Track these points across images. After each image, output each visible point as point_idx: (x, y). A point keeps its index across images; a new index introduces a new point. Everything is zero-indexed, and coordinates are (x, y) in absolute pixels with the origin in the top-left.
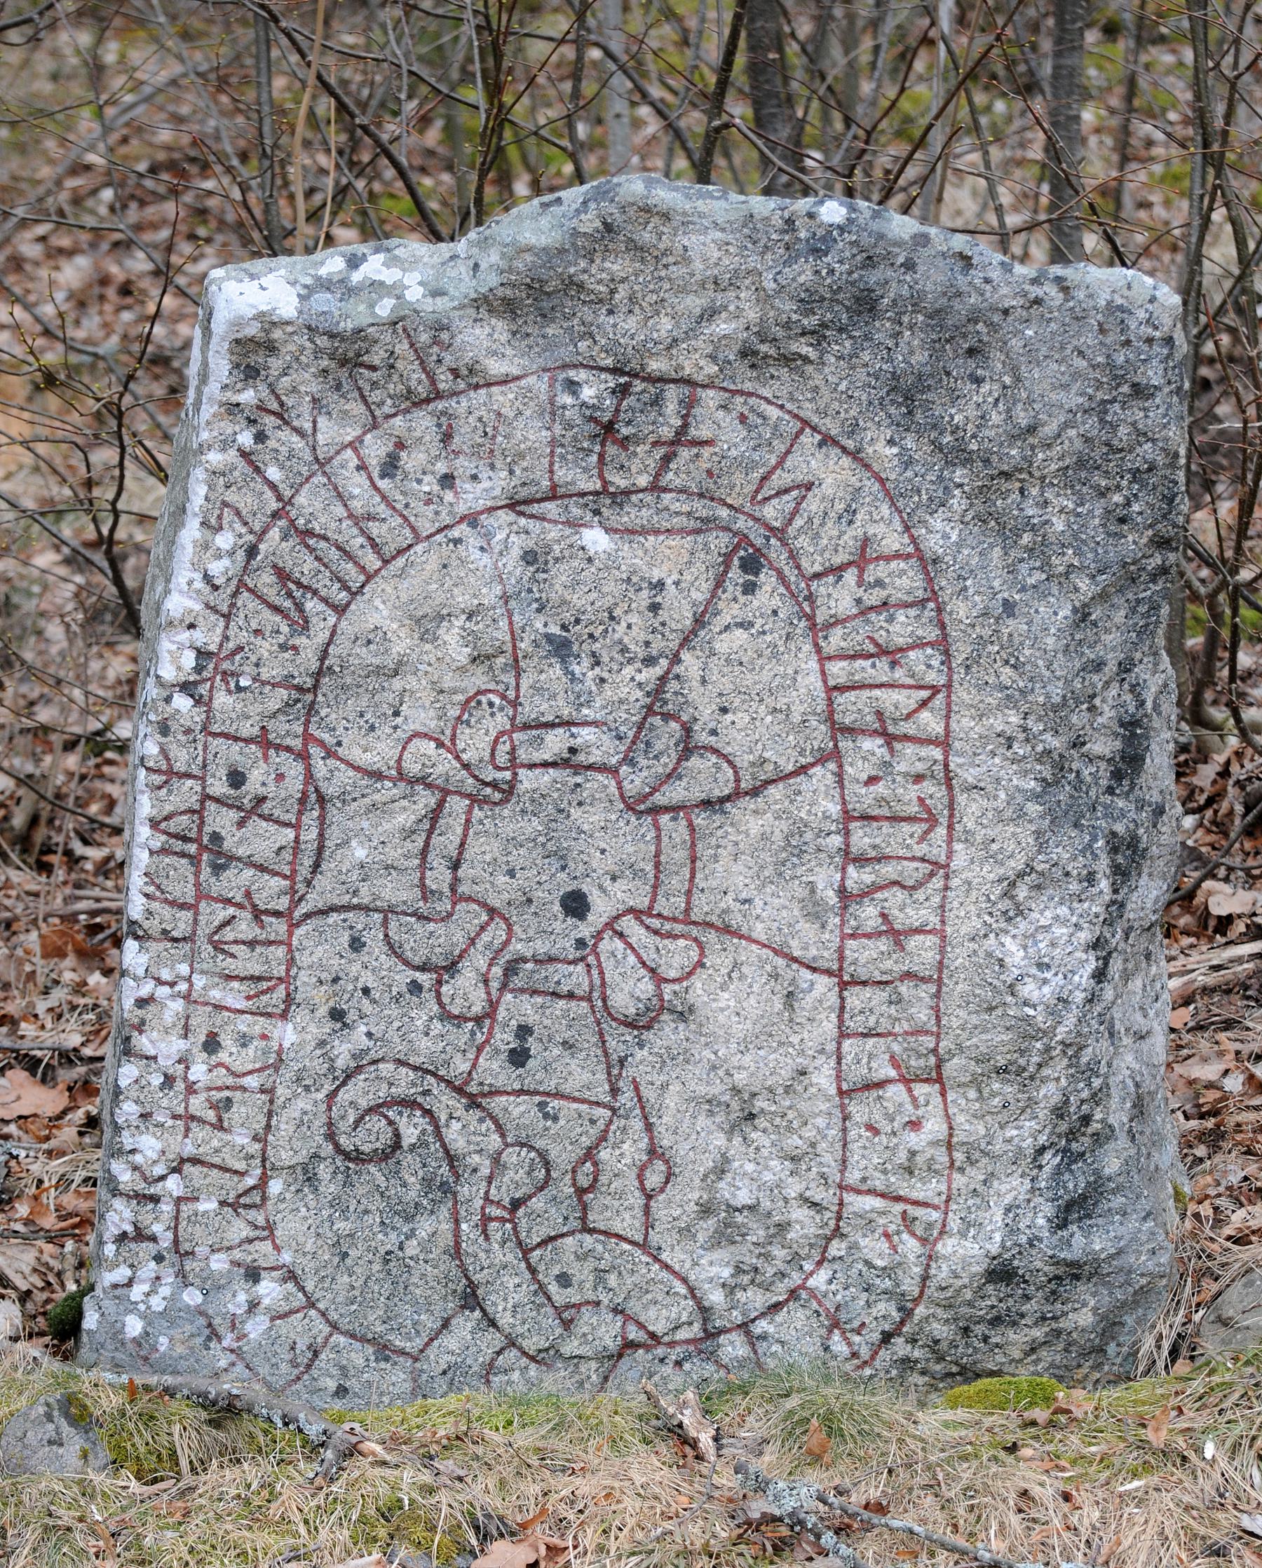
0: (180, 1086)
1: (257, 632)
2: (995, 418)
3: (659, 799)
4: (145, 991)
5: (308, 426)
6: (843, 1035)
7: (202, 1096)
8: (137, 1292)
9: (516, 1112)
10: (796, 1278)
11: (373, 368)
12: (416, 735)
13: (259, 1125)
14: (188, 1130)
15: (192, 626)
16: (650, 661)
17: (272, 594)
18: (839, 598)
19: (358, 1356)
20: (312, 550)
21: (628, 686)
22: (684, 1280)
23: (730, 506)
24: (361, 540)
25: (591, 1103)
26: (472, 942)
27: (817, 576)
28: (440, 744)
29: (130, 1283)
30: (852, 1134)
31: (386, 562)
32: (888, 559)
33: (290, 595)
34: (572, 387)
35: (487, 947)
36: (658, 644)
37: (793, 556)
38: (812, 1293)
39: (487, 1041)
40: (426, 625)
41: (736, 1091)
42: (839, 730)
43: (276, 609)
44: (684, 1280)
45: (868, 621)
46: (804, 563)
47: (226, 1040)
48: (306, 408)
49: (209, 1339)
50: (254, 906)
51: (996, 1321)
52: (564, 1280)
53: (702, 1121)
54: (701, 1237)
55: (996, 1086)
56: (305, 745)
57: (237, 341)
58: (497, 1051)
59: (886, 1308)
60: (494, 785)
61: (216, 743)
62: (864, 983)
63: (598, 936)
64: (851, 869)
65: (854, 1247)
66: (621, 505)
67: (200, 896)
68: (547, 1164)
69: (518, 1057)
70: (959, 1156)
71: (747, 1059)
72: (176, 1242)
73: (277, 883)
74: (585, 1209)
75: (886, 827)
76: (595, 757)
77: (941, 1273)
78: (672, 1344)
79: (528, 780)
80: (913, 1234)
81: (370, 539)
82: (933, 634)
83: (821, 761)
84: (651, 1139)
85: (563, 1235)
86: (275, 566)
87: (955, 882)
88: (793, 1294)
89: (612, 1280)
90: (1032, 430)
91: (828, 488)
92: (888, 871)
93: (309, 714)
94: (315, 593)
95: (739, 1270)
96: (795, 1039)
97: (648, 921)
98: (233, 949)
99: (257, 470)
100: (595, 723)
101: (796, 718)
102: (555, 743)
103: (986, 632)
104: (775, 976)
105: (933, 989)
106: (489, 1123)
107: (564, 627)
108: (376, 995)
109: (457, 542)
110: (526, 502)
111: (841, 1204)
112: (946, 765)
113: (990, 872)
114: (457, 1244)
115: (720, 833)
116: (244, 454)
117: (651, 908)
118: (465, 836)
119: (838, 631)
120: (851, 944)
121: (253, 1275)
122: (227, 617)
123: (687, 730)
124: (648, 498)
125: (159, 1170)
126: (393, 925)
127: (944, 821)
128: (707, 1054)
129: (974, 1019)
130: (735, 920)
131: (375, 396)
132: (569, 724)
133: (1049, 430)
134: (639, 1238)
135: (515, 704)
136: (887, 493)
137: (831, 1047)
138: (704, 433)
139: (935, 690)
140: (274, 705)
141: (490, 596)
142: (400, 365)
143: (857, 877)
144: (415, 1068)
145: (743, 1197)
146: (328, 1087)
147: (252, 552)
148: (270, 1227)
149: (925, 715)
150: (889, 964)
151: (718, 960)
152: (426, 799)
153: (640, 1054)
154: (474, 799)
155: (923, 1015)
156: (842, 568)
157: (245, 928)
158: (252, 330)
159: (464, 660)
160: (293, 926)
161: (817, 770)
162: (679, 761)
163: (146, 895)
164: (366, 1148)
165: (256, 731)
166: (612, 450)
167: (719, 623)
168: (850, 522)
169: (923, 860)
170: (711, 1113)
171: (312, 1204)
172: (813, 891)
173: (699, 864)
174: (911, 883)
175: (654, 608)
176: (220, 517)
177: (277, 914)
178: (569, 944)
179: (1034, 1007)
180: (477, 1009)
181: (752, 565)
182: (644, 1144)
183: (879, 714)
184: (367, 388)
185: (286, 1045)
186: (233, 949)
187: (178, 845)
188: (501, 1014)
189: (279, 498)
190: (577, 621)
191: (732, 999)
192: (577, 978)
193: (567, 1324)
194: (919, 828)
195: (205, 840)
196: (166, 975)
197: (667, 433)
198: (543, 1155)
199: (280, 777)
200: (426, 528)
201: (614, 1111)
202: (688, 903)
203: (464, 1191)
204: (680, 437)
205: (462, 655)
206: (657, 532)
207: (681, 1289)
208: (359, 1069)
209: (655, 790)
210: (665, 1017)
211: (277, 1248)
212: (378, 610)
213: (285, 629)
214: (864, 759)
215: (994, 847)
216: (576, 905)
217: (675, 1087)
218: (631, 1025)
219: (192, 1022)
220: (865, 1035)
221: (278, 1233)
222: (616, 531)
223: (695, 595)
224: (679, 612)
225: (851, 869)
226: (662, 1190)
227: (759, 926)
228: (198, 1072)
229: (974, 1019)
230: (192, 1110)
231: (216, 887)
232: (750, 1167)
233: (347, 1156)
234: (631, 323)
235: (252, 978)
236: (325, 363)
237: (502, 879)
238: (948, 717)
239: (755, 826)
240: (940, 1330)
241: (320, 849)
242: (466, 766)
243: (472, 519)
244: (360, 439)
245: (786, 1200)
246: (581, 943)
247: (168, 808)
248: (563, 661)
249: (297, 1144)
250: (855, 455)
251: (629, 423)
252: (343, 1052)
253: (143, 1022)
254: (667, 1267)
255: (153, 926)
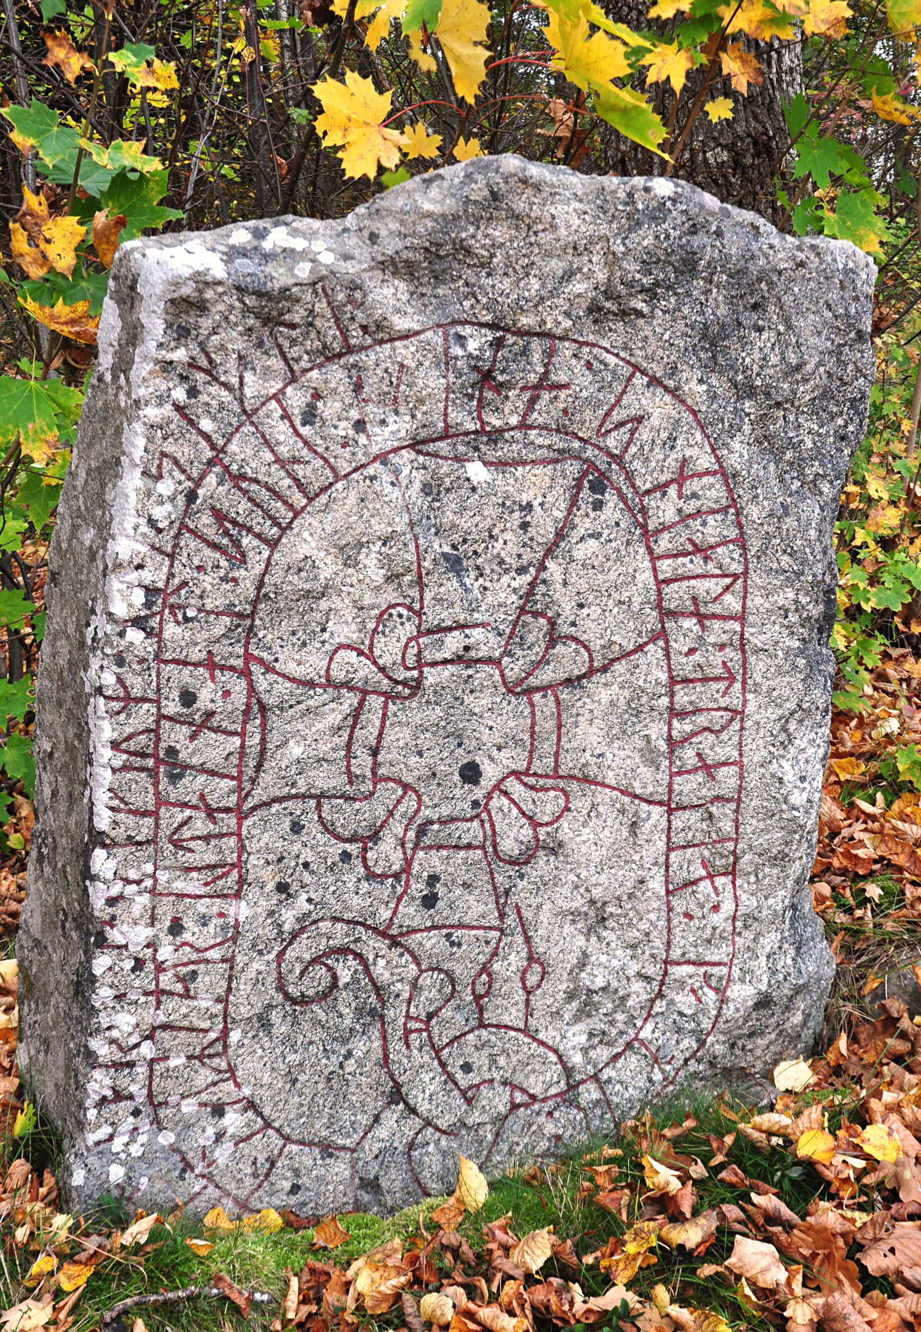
0: (150, 966)
1: (200, 568)
2: (774, 359)
3: (533, 681)
4: (115, 891)
5: (235, 381)
6: (670, 849)
7: (170, 973)
8: (117, 1145)
9: (428, 945)
10: (632, 1033)
11: (293, 326)
12: (341, 646)
13: (221, 991)
14: (159, 1003)
15: (140, 567)
16: (521, 570)
17: (211, 533)
18: (665, 509)
19: (307, 1158)
20: (245, 492)
21: (505, 591)
22: (555, 1051)
23: (581, 439)
24: (288, 481)
25: (485, 928)
26: (391, 813)
27: (648, 492)
28: (360, 653)
29: (111, 1138)
30: (675, 922)
31: (311, 500)
32: (700, 475)
33: (226, 533)
34: (461, 340)
35: (403, 815)
36: (527, 556)
37: (630, 477)
38: (642, 1043)
39: (405, 892)
40: (349, 553)
41: (592, 902)
42: (666, 614)
43: (215, 546)
44: (555, 1051)
45: (687, 526)
46: (638, 483)
47: (188, 923)
48: (232, 363)
49: (184, 1171)
50: (207, 806)
51: (752, 1035)
52: (467, 1068)
53: (568, 929)
54: (567, 1017)
55: (767, 870)
56: (246, 663)
57: (172, 301)
58: (413, 899)
59: (689, 1043)
60: (404, 683)
61: (167, 669)
62: (685, 808)
63: (489, 797)
64: (675, 723)
65: (671, 1002)
66: (495, 442)
67: (161, 801)
68: (453, 982)
69: (429, 901)
70: (739, 924)
71: (603, 878)
72: (150, 1095)
73: (226, 784)
74: (481, 1010)
75: (699, 687)
76: (483, 652)
77: (729, 1011)
78: (544, 1100)
79: (432, 676)
80: (710, 986)
81: (296, 480)
82: (733, 533)
83: (653, 640)
84: (529, 948)
85: (465, 1034)
86: (213, 508)
87: (748, 724)
88: (629, 1045)
89: (502, 1061)
90: (798, 368)
91: (655, 421)
92: (702, 720)
93: (248, 637)
94: (249, 530)
95: (591, 1035)
96: (636, 857)
97: (526, 779)
98: (191, 844)
99: (191, 422)
100: (483, 625)
101: (636, 607)
102: (453, 643)
103: (771, 529)
104: (622, 811)
105: (733, 806)
106: (407, 956)
107: (454, 547)
108: (314, 867)
109: (373, 478)
110: (424, 442)
111: (666, 973)
112: (742, 634)
113: (773, 713)
114: (386, 1056)
115: (579, 704)
116: (178, 408)
117: (528, 768)
118: (383, 726)
119: (666, 535)
120: (678, 779)
121: (218, 1111)
122: (172, 556)
123: (552, 624)
124: (518, 435)
125: (133, 1040)
126: (326, 807)
127: (739, 678)
128: (571, 877)
129: (761, 825)
130: (592, 771)
131: (294, 352)
132: (461, 627)
133: (809, 367)
134: (521, 1025)
135: (419, 614)
136: (698, 422)
137: (662, 860)
138: (563, 378)
139: (736, 577)
140: (219, 631)
141: (401, 524)
142: (318, 322)
143: (680, 727)
144: (348, 922)
145: (600, 982)
146: (277, 949)
147: (191, 496)
148: (232, 1070)
149: (728, 597)
150: (704, 791)
151: (580, 804)
152: (350, 700)
153: (521, 884)
154: (389, 696)
155: (727, 826)
156: (667, 484)
157: (201, 826)
158: (187, 290)
159: (381, 581)
160: (242, 817)
161: (650, 647)
162: (547, 649)
163: (112, 809)
164: (311, 992)
165: (204, 655)
166: (489, 395)
167: (575, 535)
168: (673, 448)
169: (726, 709)
170: (574, 922)
171: (267, 1045)
172: (649, 742)
173: (564, 730)
174: (718, 727)
175: (525, 526)
176: (160, 467)
177: (227, 810)
178: (467, 805)
179: (797, 809)
180: (396, 867)
181: (598, 487)
182: (524, 955)
183: (694, 599)
184: (286, 344)
185: (241, 919)
186: (191, 844)
187: (138, 762)
188: (416, 868)
189: (213, 447)
190: (465, 541)
191: (591, 835)
192: (473, 831)
193: (469, 1101)
194: (722, 685)
195: (161, 755)
196: (133, 875)
197: (533, 378)
198: (449, 974)
199: (227, 694)
200: (344, 467)
201: (502, 931)
202: (556, 762)
203: (390, 1013)
204: (544, 383)
205: (377, 575)
206: (524, 463)
207: (553, 1058)
208: (303, 929)
209: (529, 674)
210: (541, 853)
211: (238, 1085)
212: (307, 541)
213: (224, 563)
214: (685, 635)
215: (775, 694)
216: (471, 773)
217: (547, 906)
218: (513, 862)
219: (159, 911)
220: (684, 847)
221: (239, 1073)
222: (491, 464)
223: (556, 513)
224: (544, 526)
225: (675, 723)
226: (539, 986)
227: (611, 774)
228: (165, 953)
229: (761, 825)
230: (162, 985)
231: (173, 794)
232: (604, 959)
233: (294, 1001)
234: (506, 284)
235: (208, 867)
236: (251, 322)
237: (414, 759)
238: (745, 597)
239: (604, 696)
240: (719, 1049)
241: (263, 751)
242: (382, 669)
243: (382, 458)
244: (282, 391)
245: (628, 979)
246: (476, 804)
247: (128, 730)
248: (459, 576)
249: (254, 1000)
250: (673, 392)
251: (503, 372)
252: (288, 918)
253: (113, 918)
254: (542, 1043)
255: (119, 834)
